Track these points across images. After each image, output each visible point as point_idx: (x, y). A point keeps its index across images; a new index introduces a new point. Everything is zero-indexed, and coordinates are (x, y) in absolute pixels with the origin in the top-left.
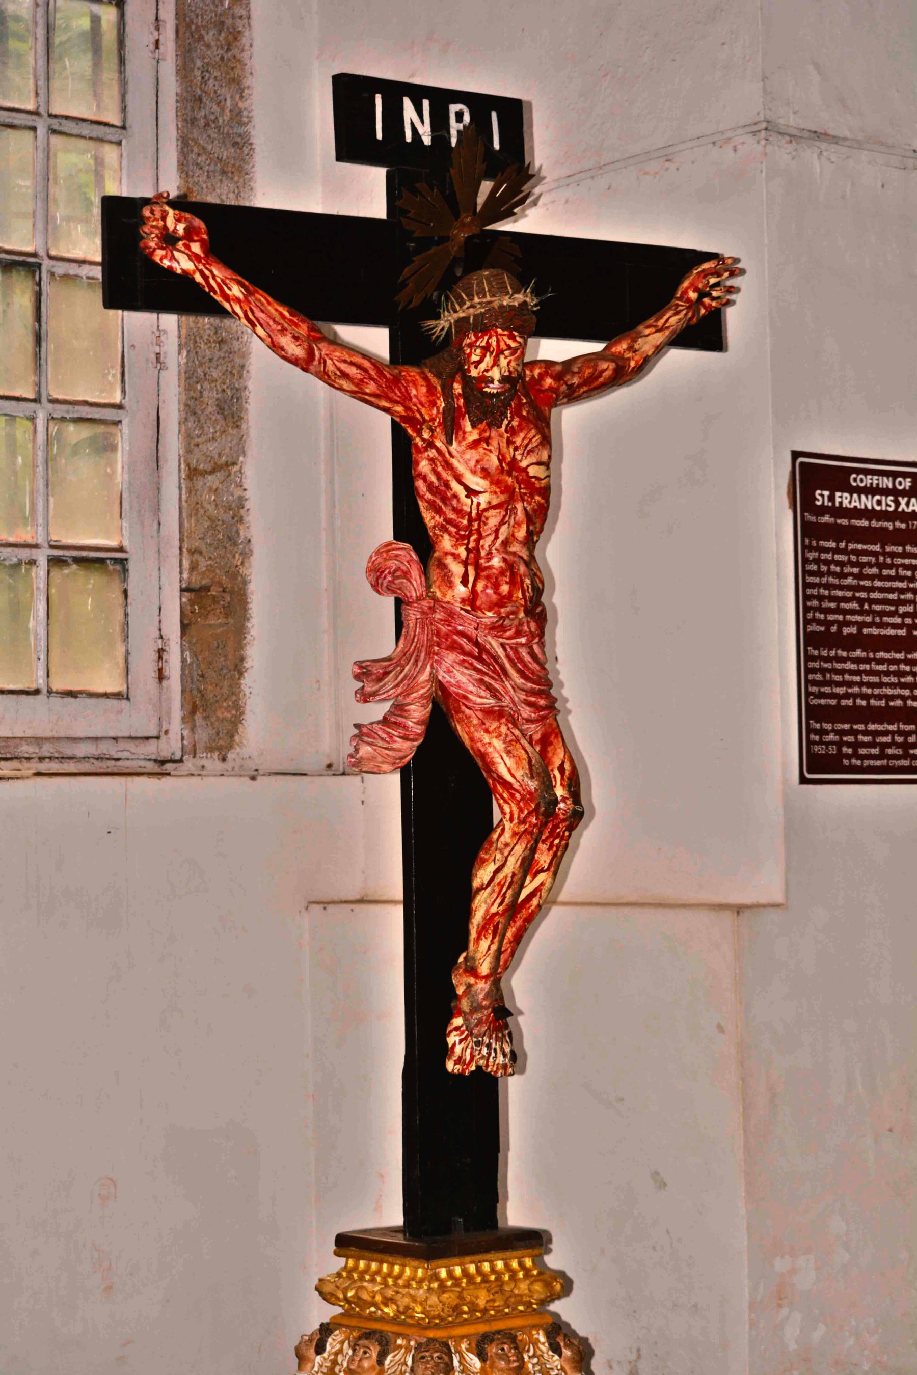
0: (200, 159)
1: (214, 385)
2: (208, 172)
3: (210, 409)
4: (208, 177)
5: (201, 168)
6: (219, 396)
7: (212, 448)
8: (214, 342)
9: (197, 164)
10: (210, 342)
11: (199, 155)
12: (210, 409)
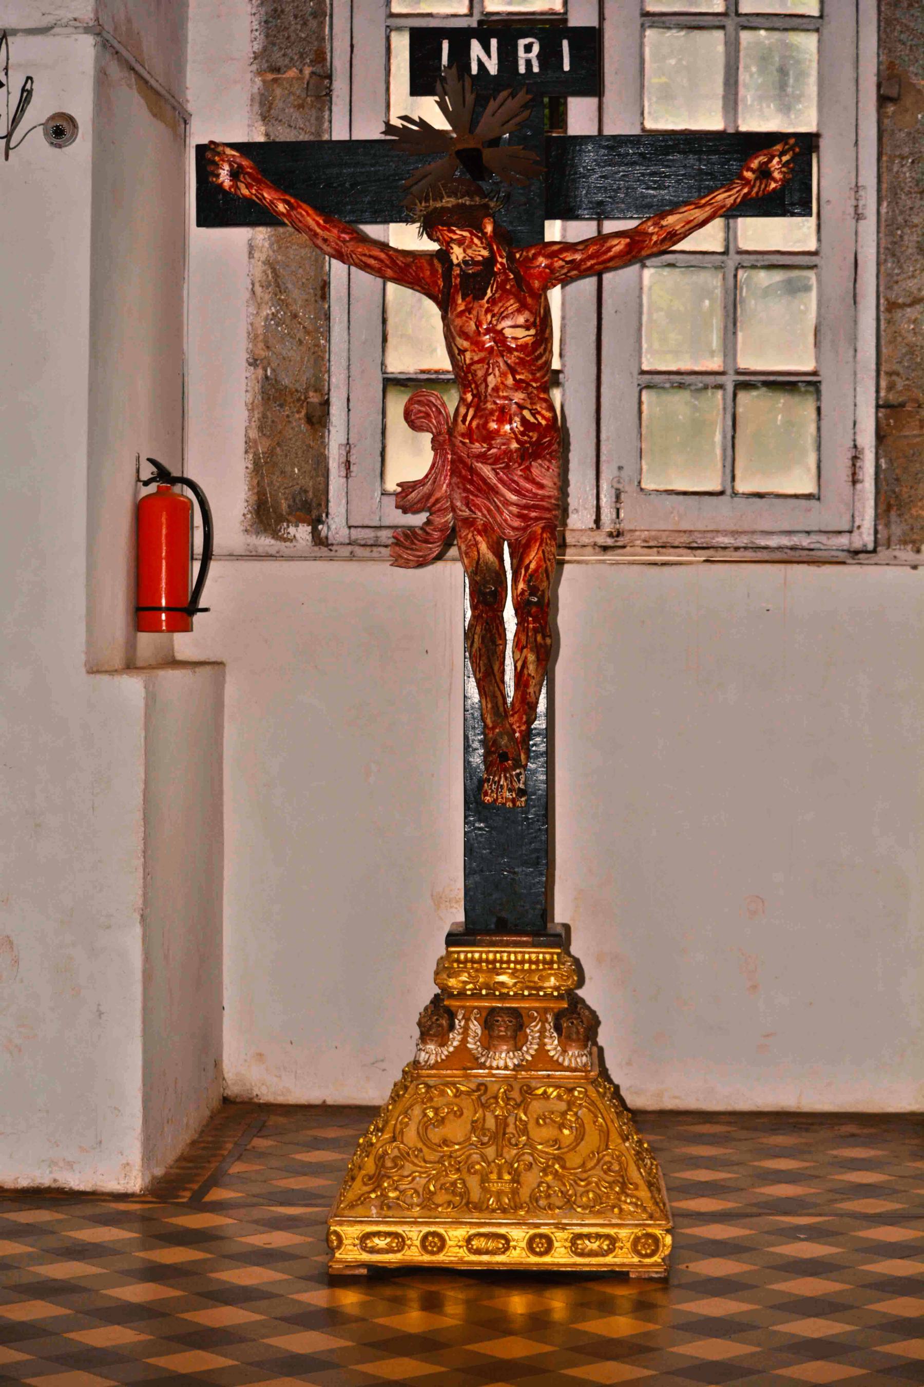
0: (902, 36)
1: (914, 230)
2: (911, 46)
3: (910, 251)
4: (911, 50)
5: (904, 44)
6: (919, 239)
7: (912, 284)
8: (915, 192)
9: (900, 41)
10: (911, 193)
11: (901, 32)
12: (910, 251)
